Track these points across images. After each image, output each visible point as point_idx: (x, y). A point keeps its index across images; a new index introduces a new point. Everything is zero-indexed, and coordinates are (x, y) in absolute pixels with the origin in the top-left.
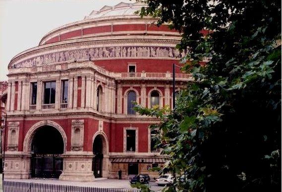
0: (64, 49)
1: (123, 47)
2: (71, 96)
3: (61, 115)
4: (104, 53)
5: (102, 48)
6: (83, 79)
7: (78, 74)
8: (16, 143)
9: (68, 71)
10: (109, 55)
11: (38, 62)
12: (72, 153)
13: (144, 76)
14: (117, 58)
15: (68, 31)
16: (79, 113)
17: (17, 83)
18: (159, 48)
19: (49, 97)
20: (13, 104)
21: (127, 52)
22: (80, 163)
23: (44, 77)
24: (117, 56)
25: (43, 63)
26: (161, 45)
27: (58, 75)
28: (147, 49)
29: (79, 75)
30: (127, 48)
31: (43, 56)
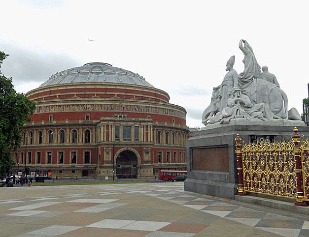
0: (111, 103)
3: (137, 145)
6: (149, 127)
8: (110, 159)
9: (140, 122)
11: (89, 108)
12: (145, 164)
13: (157, 123)
14: (142, 112)
15: (94, 87)
16: (148, 145)
17: (108, 125)
19: (127, 134)
20: (105, 137)
25: (93, 110)
26: (161, 107)
30: (147, 107)
31: (93, 105)
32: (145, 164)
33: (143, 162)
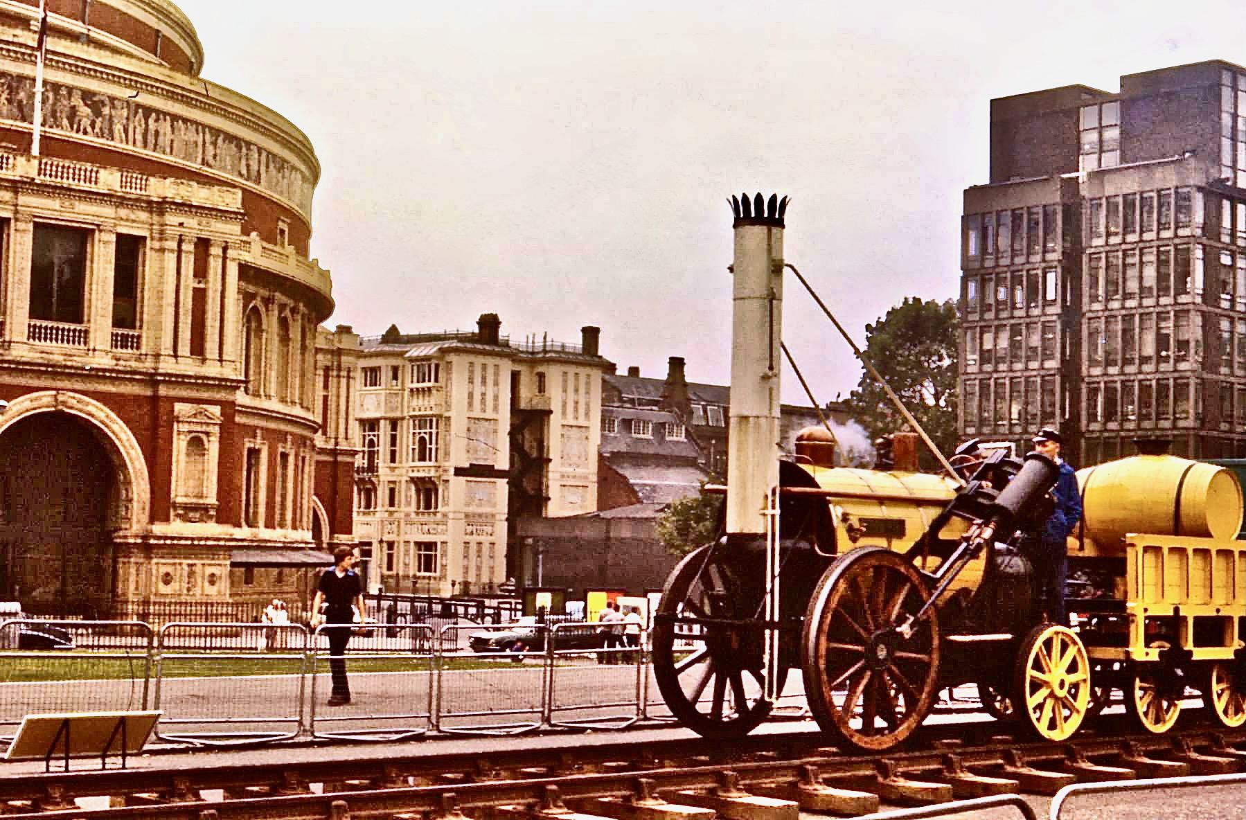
1: (138, 106)
2: (171, 310)
4: (73, 114)
5: (70, 90)
6: (215, 251)
7: (194, 225)
9: (159, 207)
10: (93, 125)
12: (176, 527)
14: (118, 145)
18: (222, 136)
21: (147, 129)
22: (204, 567)
23: (50, 208)
24: (116, 135)
27: (108, 211)
28: (197, 130)
29: (204, 235)
30: (148, 111)
32: (176, 527)
33: (161, 507)
